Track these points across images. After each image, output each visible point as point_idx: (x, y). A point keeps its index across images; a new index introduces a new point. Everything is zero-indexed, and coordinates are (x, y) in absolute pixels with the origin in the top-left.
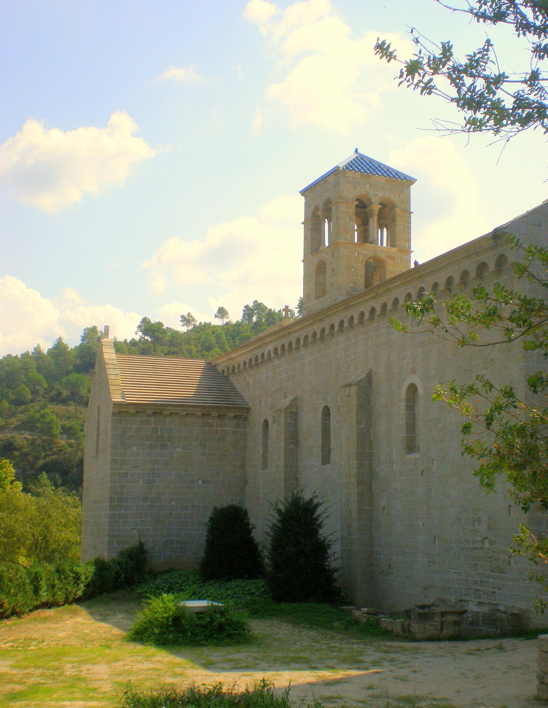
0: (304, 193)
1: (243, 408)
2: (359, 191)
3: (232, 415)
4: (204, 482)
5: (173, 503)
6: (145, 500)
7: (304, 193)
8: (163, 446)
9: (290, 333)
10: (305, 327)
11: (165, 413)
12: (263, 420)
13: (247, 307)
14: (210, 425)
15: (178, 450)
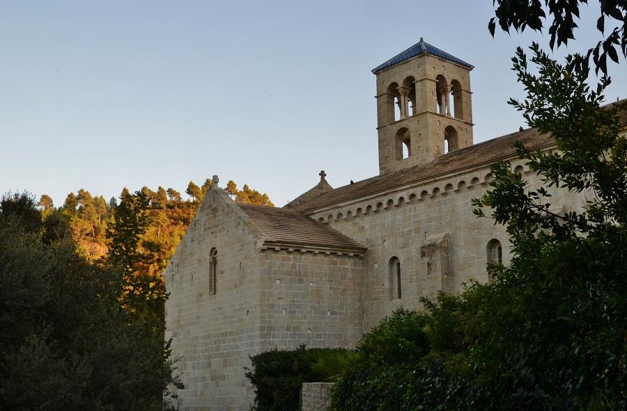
0: (377, 72)
1: (362, 249)
2: (438, 72)
3: (352, 254)
4: (333, 313)
5: (309, 331)
6: (288, 329)
7: (377, 72)
8: (301, 281)
9: (436, 181)
10: (460, 175)
11: (303, 250)
12: (388, 260)
13: (71, 196)
14: (335, 263)
15: (311, 284)
